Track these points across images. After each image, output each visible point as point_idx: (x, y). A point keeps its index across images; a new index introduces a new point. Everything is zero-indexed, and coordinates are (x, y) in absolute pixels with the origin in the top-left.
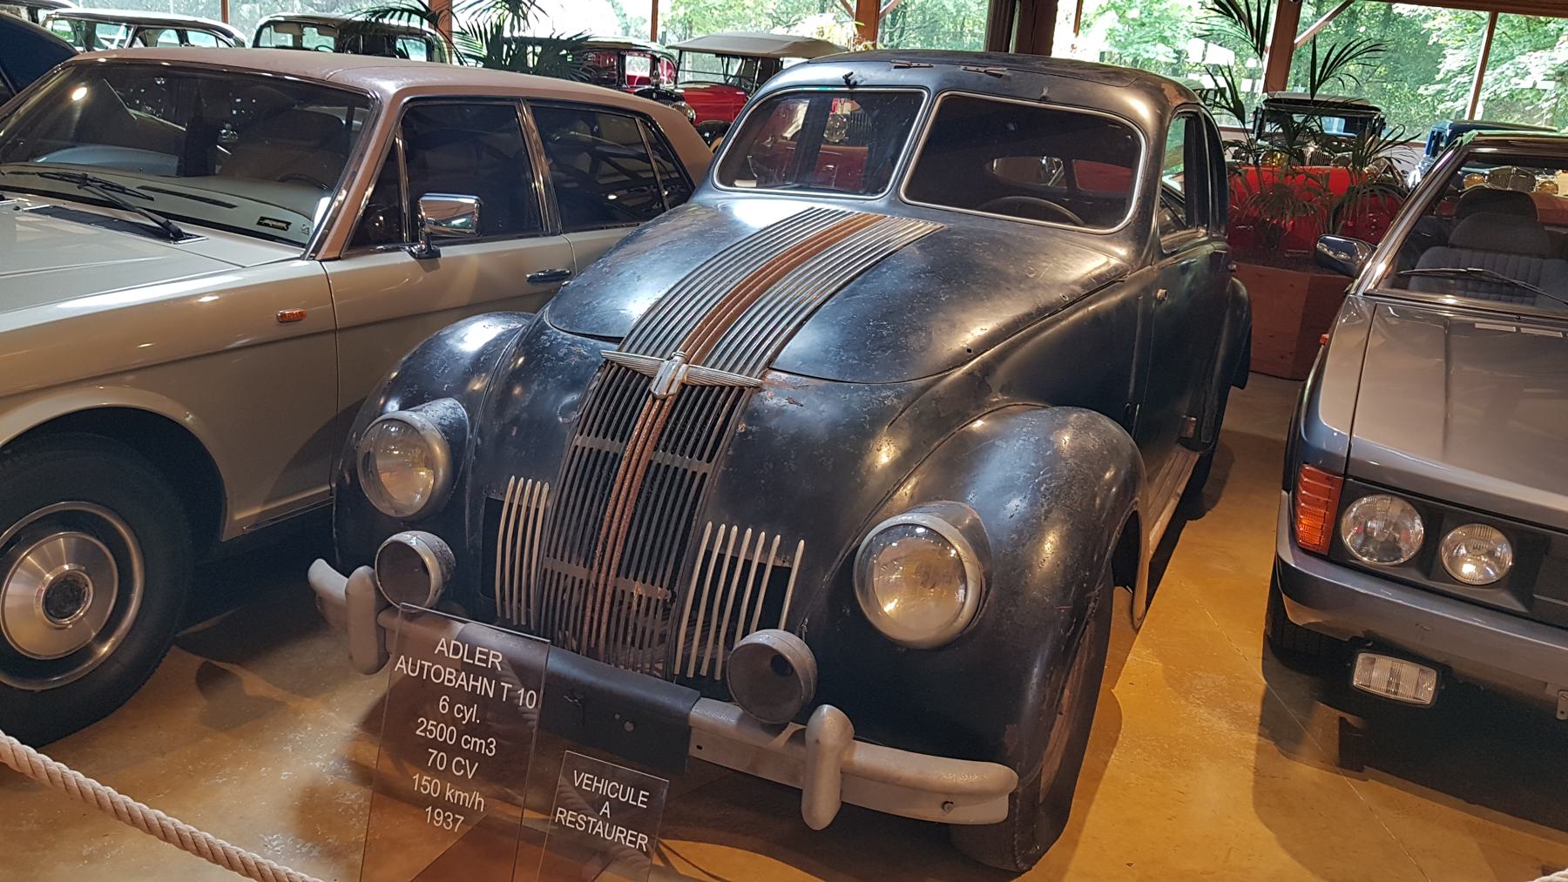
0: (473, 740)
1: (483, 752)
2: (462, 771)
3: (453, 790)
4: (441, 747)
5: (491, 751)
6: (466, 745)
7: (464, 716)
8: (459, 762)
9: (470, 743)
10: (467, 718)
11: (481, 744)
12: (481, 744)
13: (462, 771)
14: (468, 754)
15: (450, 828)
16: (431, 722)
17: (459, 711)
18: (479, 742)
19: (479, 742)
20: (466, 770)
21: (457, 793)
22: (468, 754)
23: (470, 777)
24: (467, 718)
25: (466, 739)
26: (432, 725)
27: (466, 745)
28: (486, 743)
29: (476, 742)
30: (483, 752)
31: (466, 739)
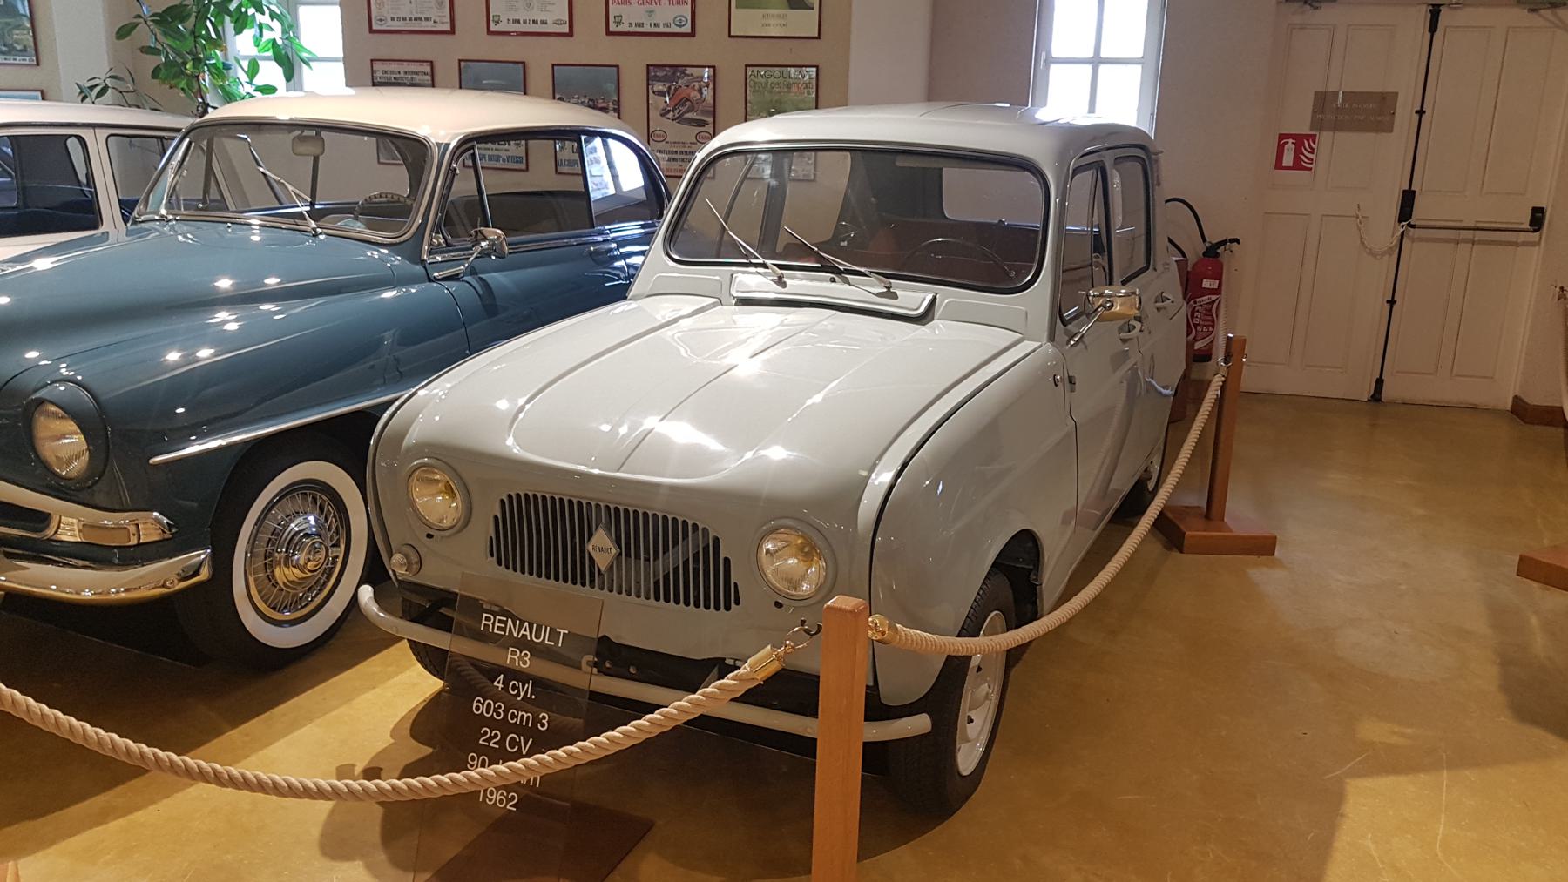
0: (520, 714)
4: (492, 724)
9: (517, 717)
11: (528, 717)
12: (528, 717)
17: (514, 687)
18: (526, 715)
19: (526, 715)
22: (518, 729)
24: (522, 694)
25: (513, 713)
29: (523, 716)
31: (513, 713)
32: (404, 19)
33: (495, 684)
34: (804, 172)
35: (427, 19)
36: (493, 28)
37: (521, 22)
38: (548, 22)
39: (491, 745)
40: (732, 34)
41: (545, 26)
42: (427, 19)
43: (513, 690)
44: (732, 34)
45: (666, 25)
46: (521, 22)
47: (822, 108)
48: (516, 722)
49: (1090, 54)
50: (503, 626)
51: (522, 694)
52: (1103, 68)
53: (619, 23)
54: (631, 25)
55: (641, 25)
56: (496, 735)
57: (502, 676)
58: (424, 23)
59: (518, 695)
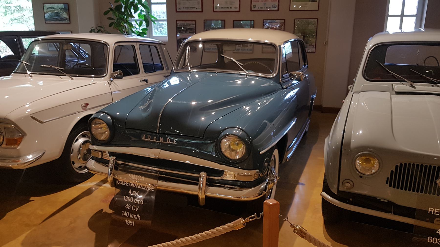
2: (135, 209)
3: (132, 215)
5: (142, 203)
7: (135, 194)
8: (134, 207)
9: (137, 201)
10: (136, 194)
11: (139, 201)
13: (135, 209)
15: (131, 225)
16: (131, 221)
20: (136, 210)
21: (133, 215)
23: (137, 210)
26: (131, 222)
27: (135, 202)
28: (141, 200)
32: (187, 8)
35: (194, 8)
36: (215, 10)
37: (224, 8)
38: (232, 8)
40: (291, 10)
41: (231, 9)
42: (194, 8)
44: (291, 10)
45: (270, 8)
46: (224, 8)
47: (285, 31)
49: (400, 13)
52: (404, 18)
53: (254, 8)
54: (258, 8)
55: (262, 8)
58: (193, 9)
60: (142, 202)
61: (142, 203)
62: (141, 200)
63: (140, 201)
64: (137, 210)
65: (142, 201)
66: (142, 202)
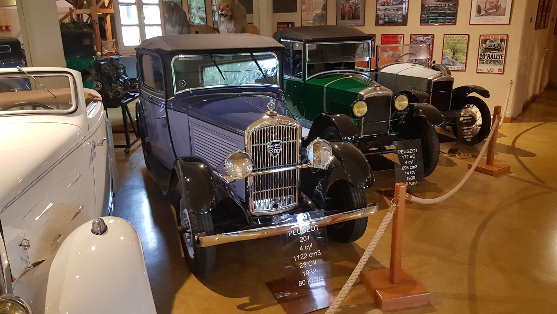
0: (313, 253)
1: (317, 255)
2: (312, 264)
6: (311, 256)
9: (312, 255)
11: (316, 254)
12: (316, 254)
13: (312, 264)
14: (312, 259)
20: (313, 264)
24: (310, 248)
27: (311, 256)
28: (317, 252)
29: (314, 254)
30: (317, 255)
33: (300, 249)
34: (462, 68)
39: (305, 258)
43: (306, 248)
48: (312, 257)
50: (296, 232)
51: (310, 248)
56: (305, 255)
57: (302, 246)
59: (309, 249)
60: (320, 252)
61: (319, 254)
62: (318, 252)
63: (316, 252)
64: (315, 264)
65: (319, 252)
66: (320, 252)
